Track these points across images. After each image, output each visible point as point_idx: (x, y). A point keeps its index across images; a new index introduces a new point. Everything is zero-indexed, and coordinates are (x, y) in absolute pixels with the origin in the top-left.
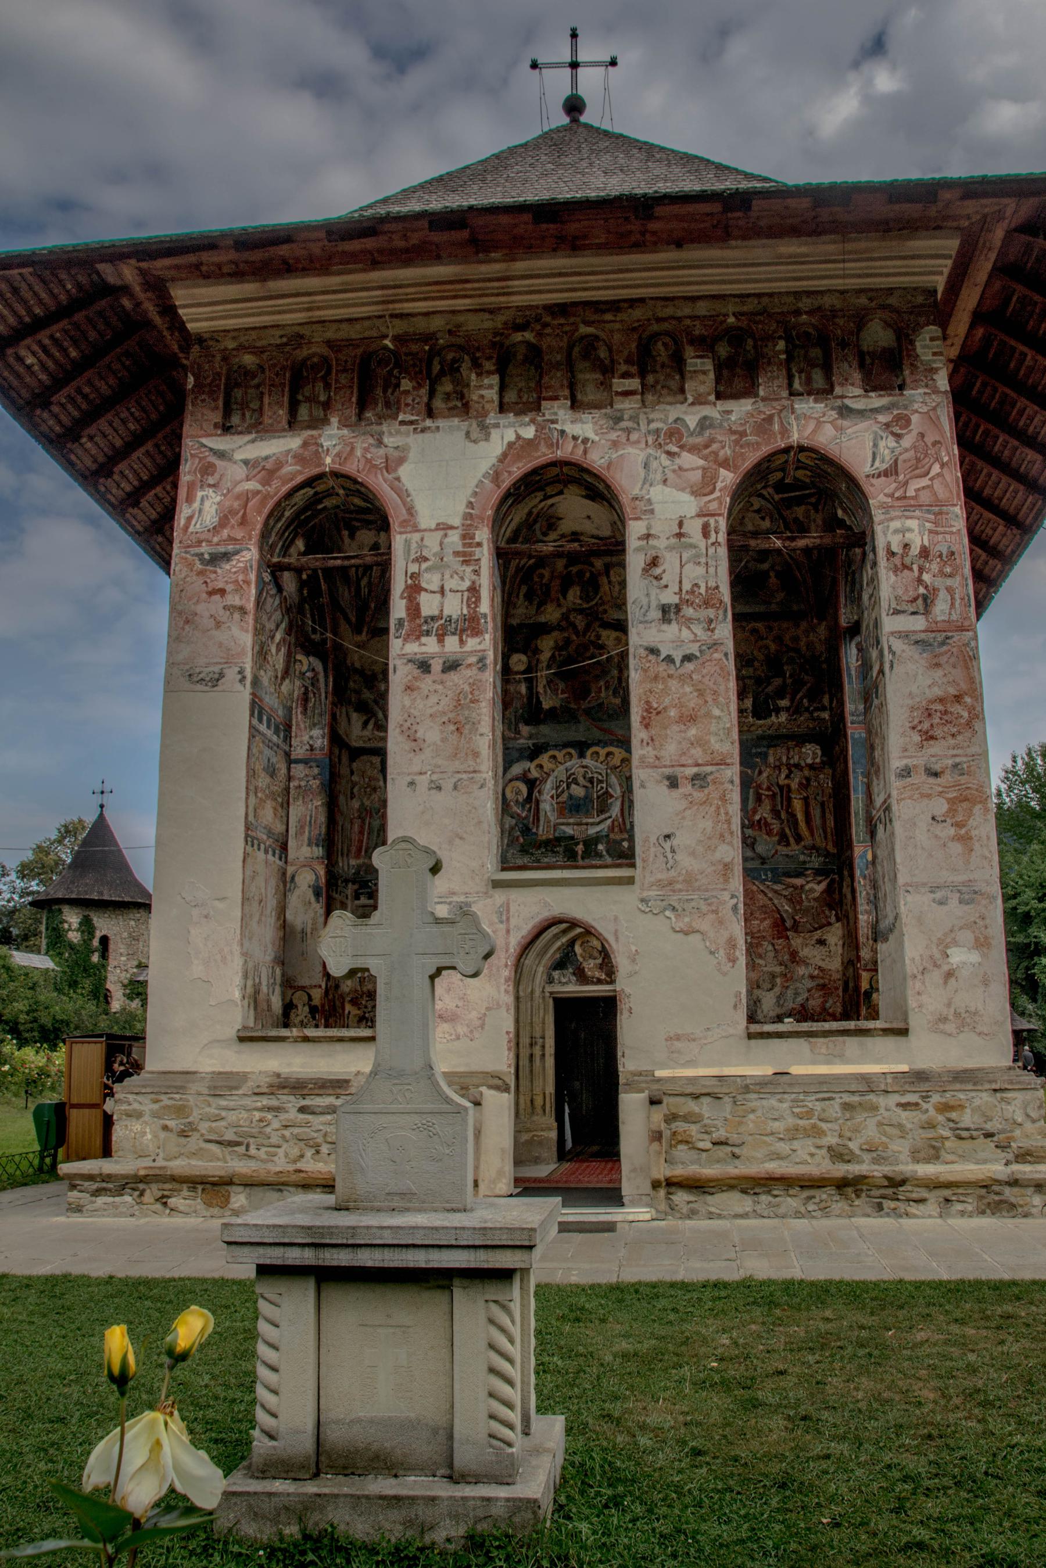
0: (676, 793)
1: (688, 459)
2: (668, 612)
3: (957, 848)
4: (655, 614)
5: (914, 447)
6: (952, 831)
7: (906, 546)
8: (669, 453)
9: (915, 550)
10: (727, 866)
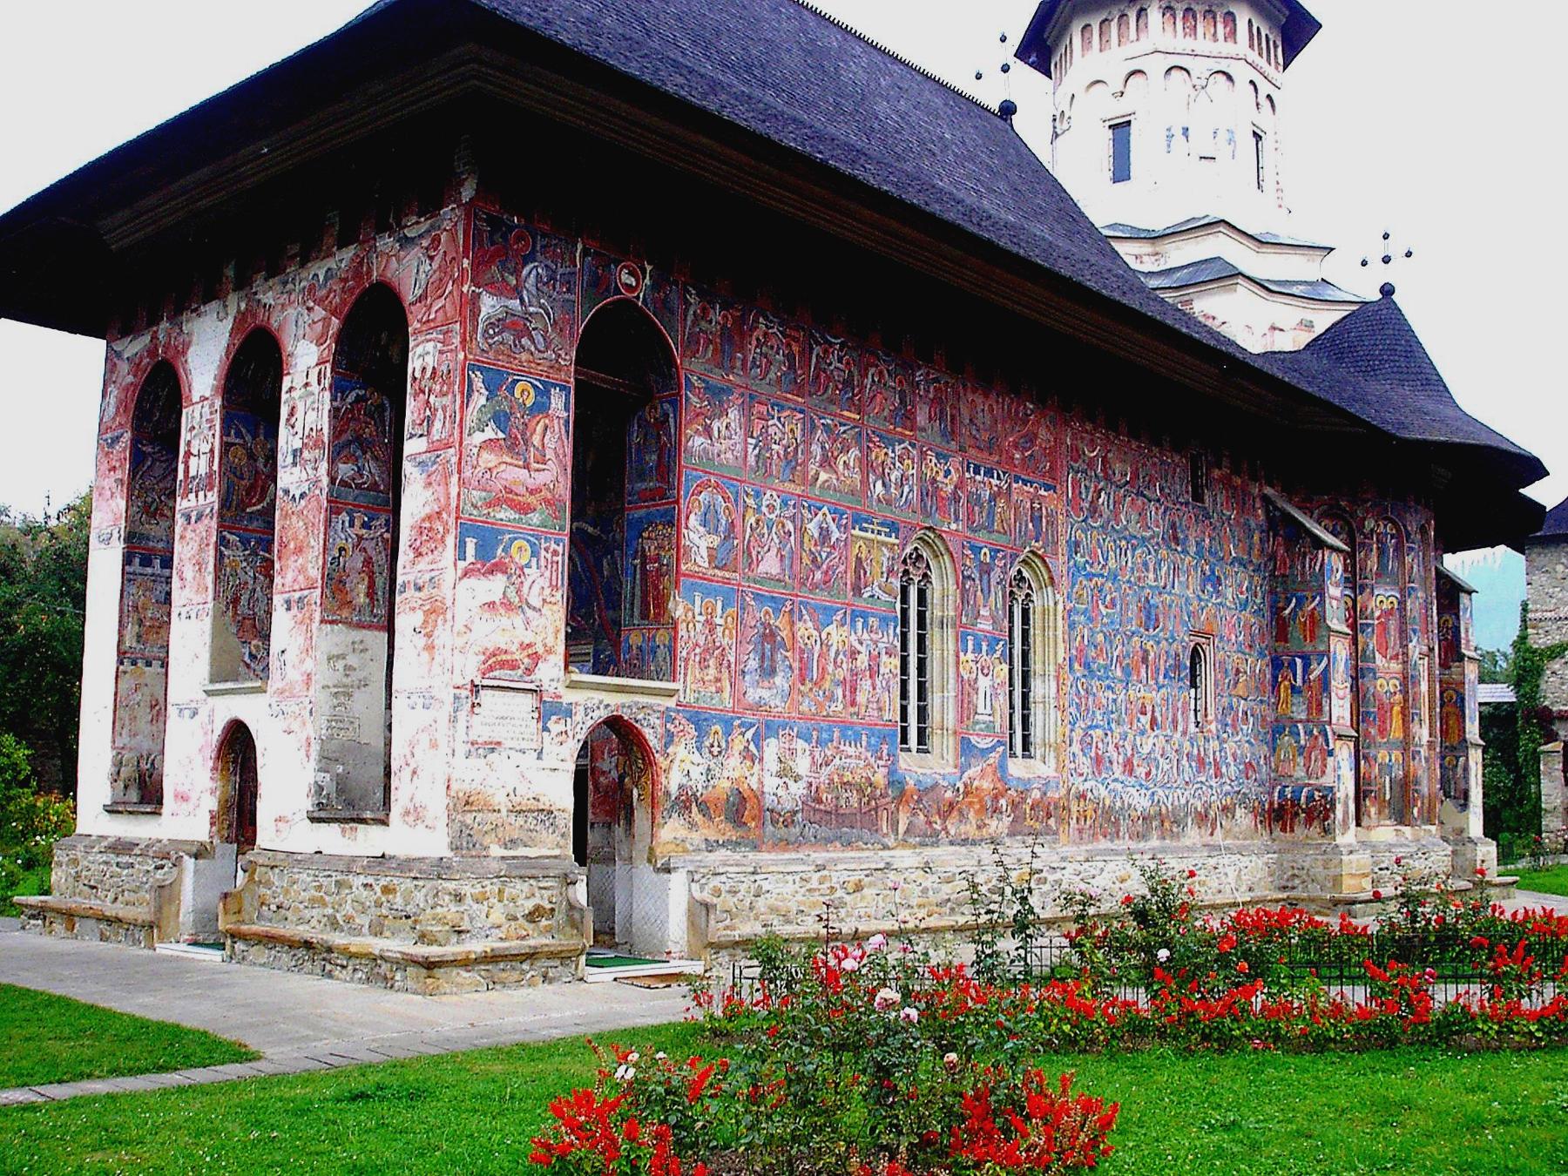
1: (319, 312)
3: (425, 655)
4: (290, 459)
8: (309, 309)
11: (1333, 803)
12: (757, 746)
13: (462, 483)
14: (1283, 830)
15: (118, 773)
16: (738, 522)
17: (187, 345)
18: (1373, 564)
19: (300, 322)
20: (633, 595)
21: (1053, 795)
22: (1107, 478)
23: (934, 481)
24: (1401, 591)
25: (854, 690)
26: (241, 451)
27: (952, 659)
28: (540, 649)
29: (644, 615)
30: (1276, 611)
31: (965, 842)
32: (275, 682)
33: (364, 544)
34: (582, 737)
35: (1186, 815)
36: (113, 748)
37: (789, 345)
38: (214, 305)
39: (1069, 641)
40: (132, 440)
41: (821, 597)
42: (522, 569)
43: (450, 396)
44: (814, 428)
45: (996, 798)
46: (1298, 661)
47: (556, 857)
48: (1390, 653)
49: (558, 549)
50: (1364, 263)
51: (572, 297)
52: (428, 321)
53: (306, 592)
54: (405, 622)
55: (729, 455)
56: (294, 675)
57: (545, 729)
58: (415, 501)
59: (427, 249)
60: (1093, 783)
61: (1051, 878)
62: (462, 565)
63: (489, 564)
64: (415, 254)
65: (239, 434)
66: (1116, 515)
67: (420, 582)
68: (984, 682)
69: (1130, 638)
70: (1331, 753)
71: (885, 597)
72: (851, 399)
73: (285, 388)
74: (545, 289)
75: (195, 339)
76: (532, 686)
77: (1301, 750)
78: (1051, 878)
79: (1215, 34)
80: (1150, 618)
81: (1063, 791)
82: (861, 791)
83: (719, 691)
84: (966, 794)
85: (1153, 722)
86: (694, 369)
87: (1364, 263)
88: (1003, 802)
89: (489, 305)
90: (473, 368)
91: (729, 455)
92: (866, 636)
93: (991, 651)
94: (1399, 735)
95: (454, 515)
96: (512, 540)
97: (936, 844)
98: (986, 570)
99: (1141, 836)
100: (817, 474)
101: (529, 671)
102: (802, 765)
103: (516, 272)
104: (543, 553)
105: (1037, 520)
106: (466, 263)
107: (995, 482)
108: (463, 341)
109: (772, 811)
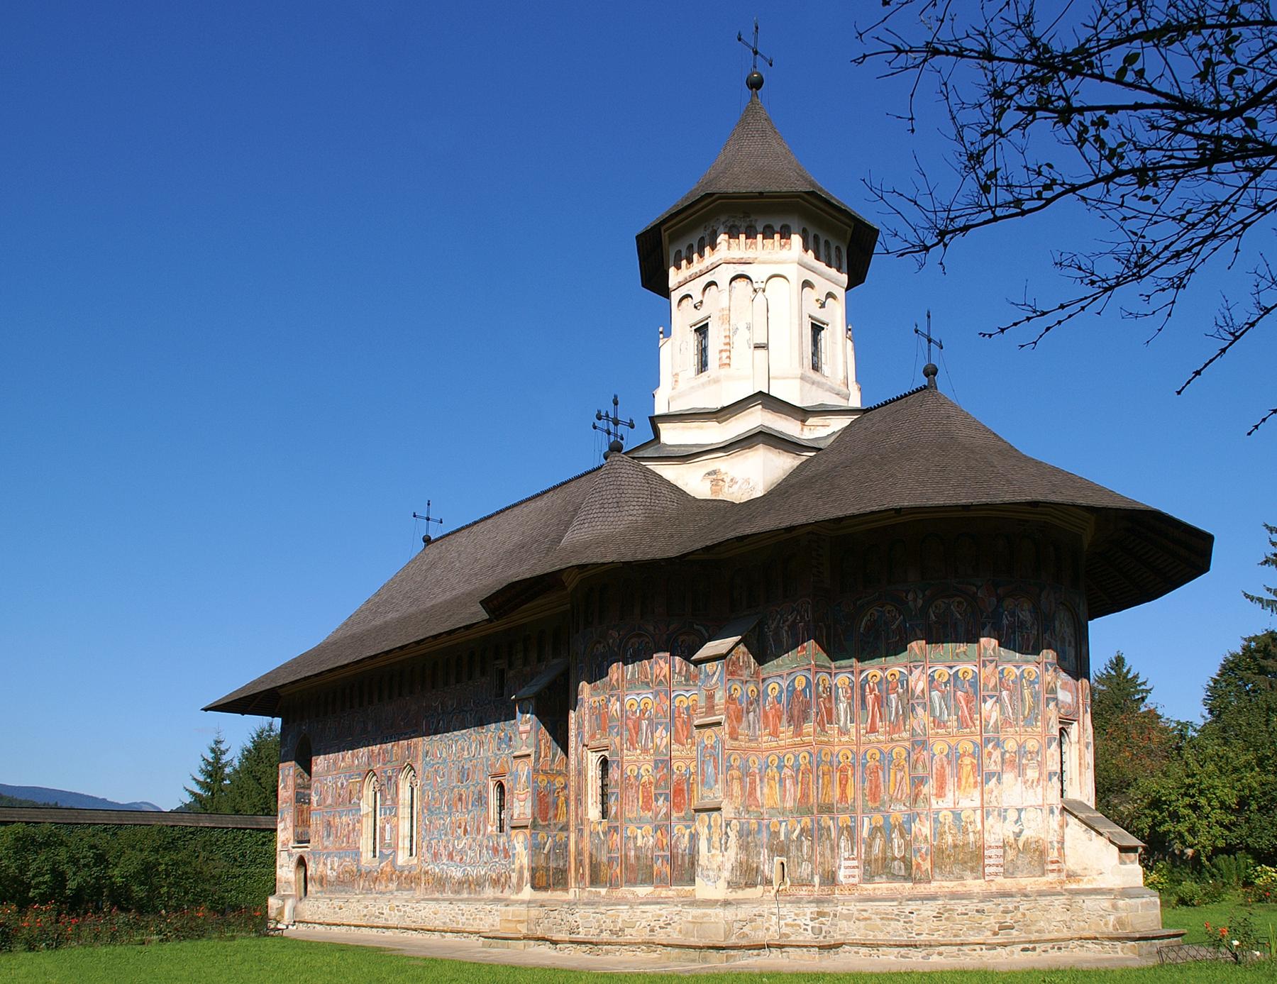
45: (392, 875)
60: (432, 866)
61: (403, 909)
68: (388, 827)
78: (403, 909)
84: (381, 873)
85: (466, 831)
97: (371, 893)
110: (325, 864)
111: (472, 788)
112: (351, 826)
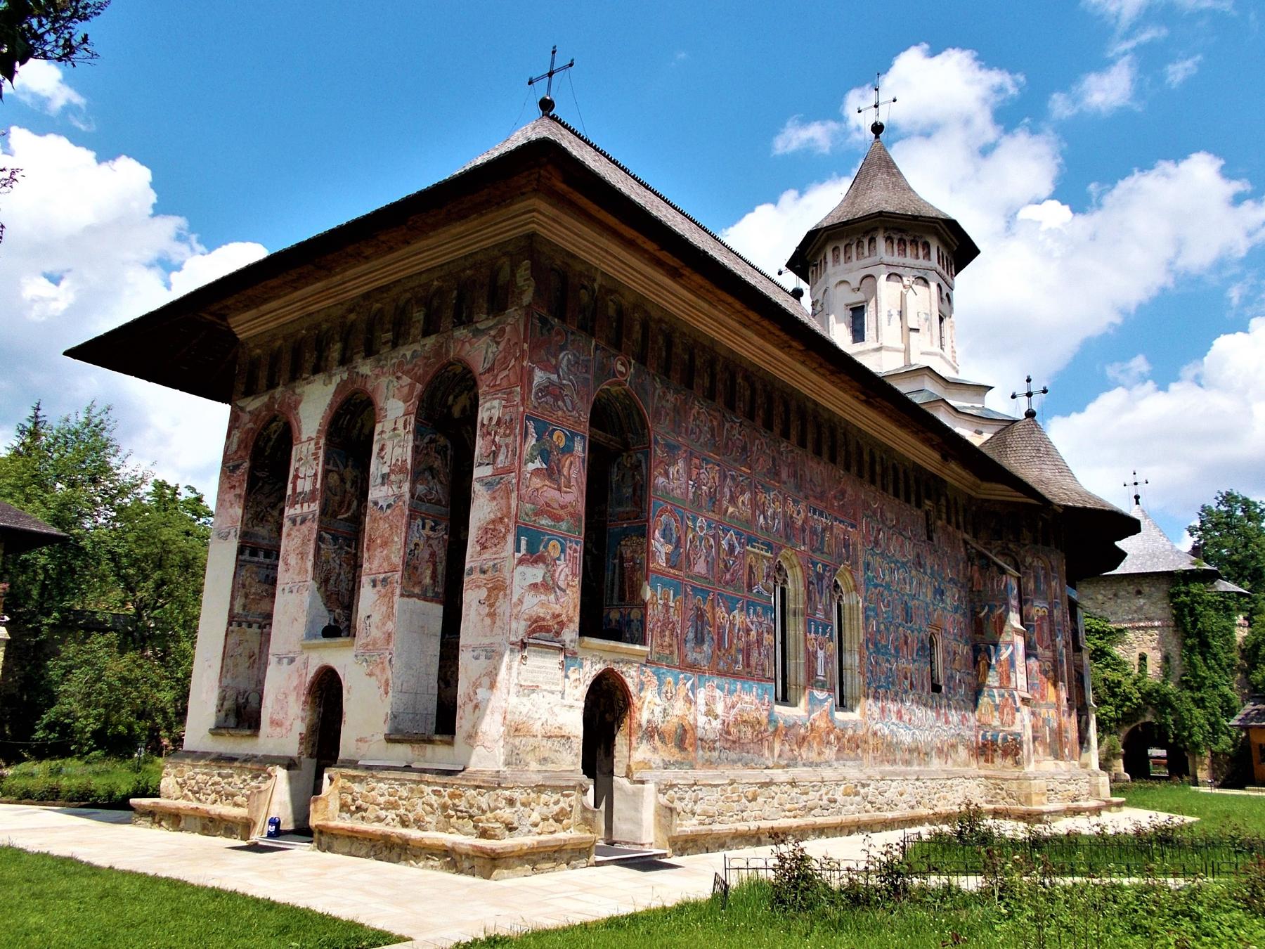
0: (375, 590)
1: (406, 380)
2: (385, 478)
3: (488, 621)
4: (379, 480)
5: (504, 349)
6: (487, 610)
7: (491, 419)
8: (398, 378)
9: (494, 422)
10: (389, 635)
11: (1021, 743)
12: (693, 693)
13: (520, 498)
14: (987, 761)
15: (222, 705)
16: (683, 538)
17: (298, 403)
18: (1031, 586)
19: (391, 386)
20: (613, 584)
21: (860, 732)
22: (883, 522)
23: (791, 517)
24: (1049, 604)
25: (748, 657)
26: (336, 477)
27: (802, 637)
28: (564, 618)
29: (622, 598)
30: (974, 614)
31: (811, 764)
32: (360, 640)
33: (431, 542)
34: (589, 683)
35: (932, 749)
36: (220, 687)
37: (711, 421)
38: (320, 377)
39: (866, 628)
40: (250, 468)
41: (729, 590)
42: (555, 560)
43: (512, 437)
44: (726, 477)
45: (828, 734)
46: (992, 647)
47: (572, 771)
48: (1045, 644)
49: (576, 548)
50: (1014, 397)
51: (589, 377)
52: (495, 385)
53: (389, 574)
54: (472, 597)
55: (679, 491)
56: (375, 633)
57: (567, 677)
58: (481, 510)
59: (494, 337)
60: (880, 725)
61: (862, 791)
62: (518, 555)
63: (534, 556)
64: (485, 339)
65: (336, 465)
66: (888, 546)
67: (485, 567)
68: (821, 654)
69: (898, 628)
70: (1018, 710)
71: (765, 593)
72: (746, 459)
73: (376, 432)
74: (572, 369)
75: (305, 399)
76: (557, 645)
77: (997, 707)
79: (917, 254)
80: (908, 617)
81: (865, 730)
82: (752, 727)
83: (672, 653)
84: (812, 730)
86: (660, 431)
87: (1014, 397)
88: (832, 737)
89: (539, 376)
90: (528, 418)
91: (679, 491)
92: (755, 619)
93: (824, 633)
94: (1054, 700)
95: (513, 519)
96: (550, 540)
97: (795, 766)
98: (820, 577)
99: (907, 763)
100: (727, 508)
101: (558, 634)
102: (719, 708)
103: (556, 357)
104: (568, 550)
105: (846, 546)
106: (526, 346)
107: (824, 520)
108: (523, 399)
109: (702, 740)
110: (690, 702)
111: (916, 632)
112: (753, 633)
